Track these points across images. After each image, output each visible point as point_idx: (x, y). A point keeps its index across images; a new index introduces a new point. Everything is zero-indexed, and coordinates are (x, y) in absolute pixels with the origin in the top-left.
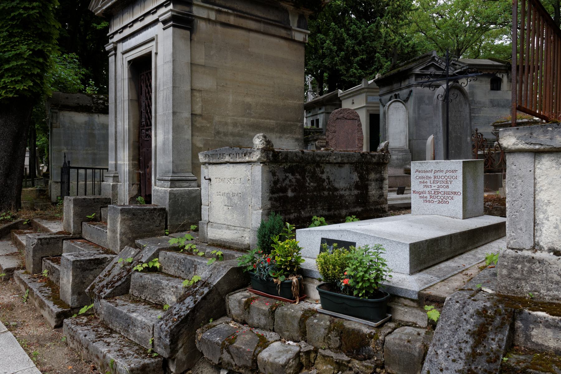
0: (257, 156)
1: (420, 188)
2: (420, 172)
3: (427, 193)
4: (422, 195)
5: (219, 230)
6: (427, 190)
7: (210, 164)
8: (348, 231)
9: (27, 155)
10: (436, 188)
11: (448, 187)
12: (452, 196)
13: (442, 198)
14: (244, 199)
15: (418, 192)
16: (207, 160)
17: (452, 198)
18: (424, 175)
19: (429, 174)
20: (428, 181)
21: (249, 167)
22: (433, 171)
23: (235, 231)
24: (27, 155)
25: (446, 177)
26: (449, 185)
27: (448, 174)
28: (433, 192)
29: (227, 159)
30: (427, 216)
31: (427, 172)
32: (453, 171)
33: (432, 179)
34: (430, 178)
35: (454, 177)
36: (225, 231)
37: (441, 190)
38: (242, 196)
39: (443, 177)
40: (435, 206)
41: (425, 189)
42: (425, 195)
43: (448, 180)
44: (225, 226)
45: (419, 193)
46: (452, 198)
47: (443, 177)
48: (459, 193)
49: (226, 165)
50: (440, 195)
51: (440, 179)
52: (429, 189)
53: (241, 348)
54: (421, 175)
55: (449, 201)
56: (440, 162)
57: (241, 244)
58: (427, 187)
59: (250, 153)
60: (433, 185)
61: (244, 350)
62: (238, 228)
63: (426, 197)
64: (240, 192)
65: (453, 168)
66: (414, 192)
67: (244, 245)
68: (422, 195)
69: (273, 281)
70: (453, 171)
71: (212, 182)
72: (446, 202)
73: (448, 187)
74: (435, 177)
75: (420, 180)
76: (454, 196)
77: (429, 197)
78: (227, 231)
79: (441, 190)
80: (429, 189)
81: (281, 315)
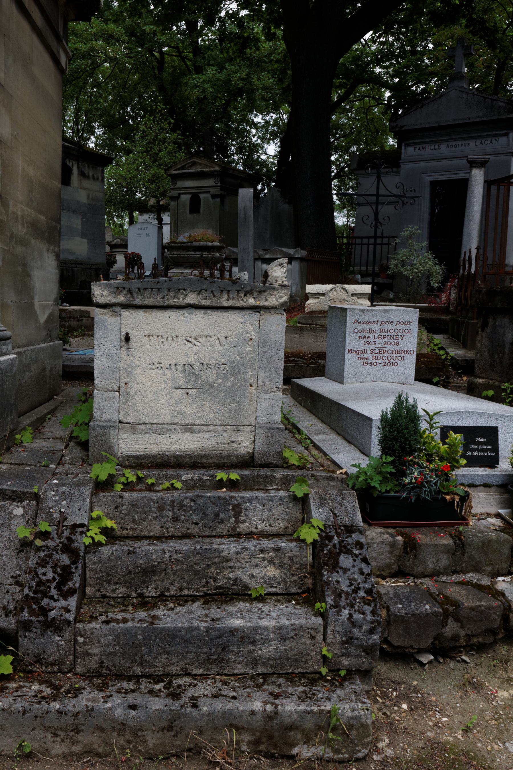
0: (281, 297)
1: (360, 346)
2: (360, 323)
3: (369, 351)
4: (361, 355)
5: (159, 437)
6: (369, 348)
7: (125, 306)
8: (469, 412)
9: (426, 305)
10: (382, 345)
11: (397, 344)
12: (403, 355)
13: (389, 358)
14: (235, 374)
15: (355, 352)
16: (122, 299)
17: (403, 359)
18: (366, 327)
19: (373, 327)
20: (371, 335)
21: (255, 316)
22: (380, 322)
23: (211, 434)
24: (426, 305)
25: (396, 331)
26: (400, 340)
27: (399, 327)
28: (377, 351)
29: (192, 298)
30: (367, 384)
31: (370, 323)
32: (406, 323)
33: (377, 334)
34: (375, 331)
35: (407, 331)
36: (180, 435)
37: (389, 347)
38: (234, 369)
39: (392, 331)
40: (379, 369)
41: (366, 347)
42: (365, 355)
43: (399, 334)
44: (175, 427)
45: (357, 352)
46: (403, 359)
47: (392, 331)
48: (412, 352)
49: (184, 312)
50: (386, 354)
51: (389, 334)
52: (372, 347)
53: (480, 606)
54: (361, 326)
55: (399, 362)
56: (390, 310)
57: (229, 456)
58: (370, 343)
59: (260, 292)
60: (378, 341)
61: (488, 607)
62: (220, 428)
63: (367, 358)
64: (223, 361)
65: (406, 319)
66: (350, 351)
67: (237, 457)
68: (361, 355)
69: (445, 499)
70: (406, 323)
71: (132, 344)
72: (393, 364)
73: (397, 344)
74: (381, 331)
75: (359, 335)
76: (405, 355)
77: (371, 358)
78: (188, 436)
79: (389, 347)
80: (372, 347)
81: (480, 544)
